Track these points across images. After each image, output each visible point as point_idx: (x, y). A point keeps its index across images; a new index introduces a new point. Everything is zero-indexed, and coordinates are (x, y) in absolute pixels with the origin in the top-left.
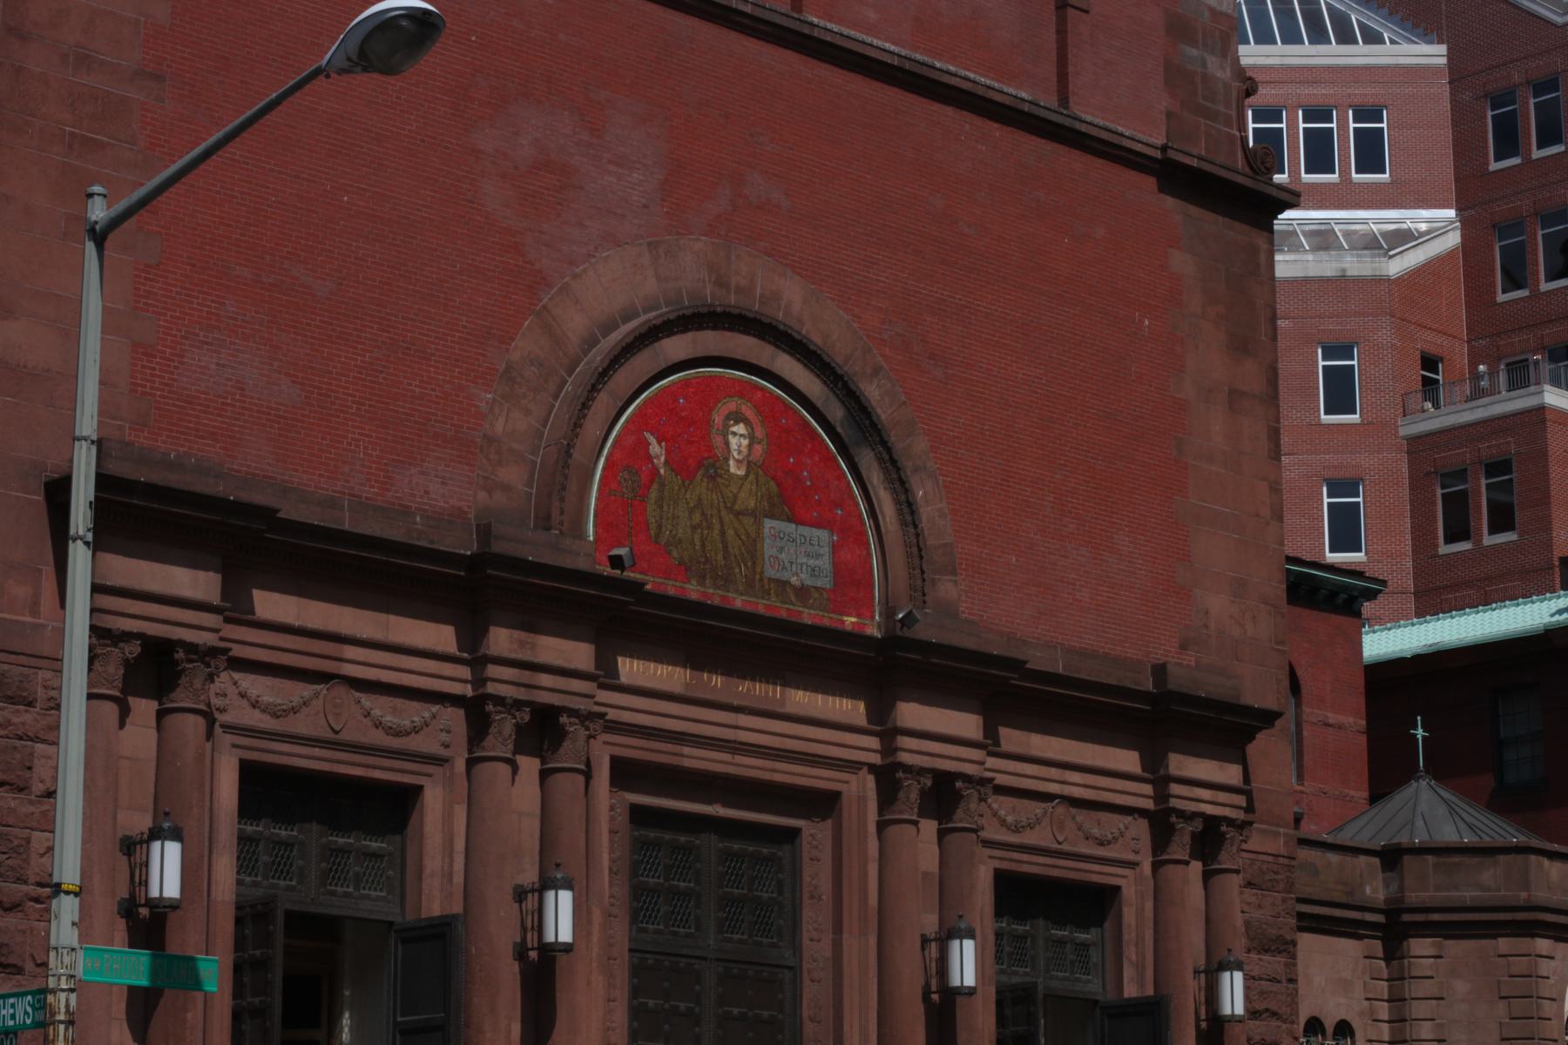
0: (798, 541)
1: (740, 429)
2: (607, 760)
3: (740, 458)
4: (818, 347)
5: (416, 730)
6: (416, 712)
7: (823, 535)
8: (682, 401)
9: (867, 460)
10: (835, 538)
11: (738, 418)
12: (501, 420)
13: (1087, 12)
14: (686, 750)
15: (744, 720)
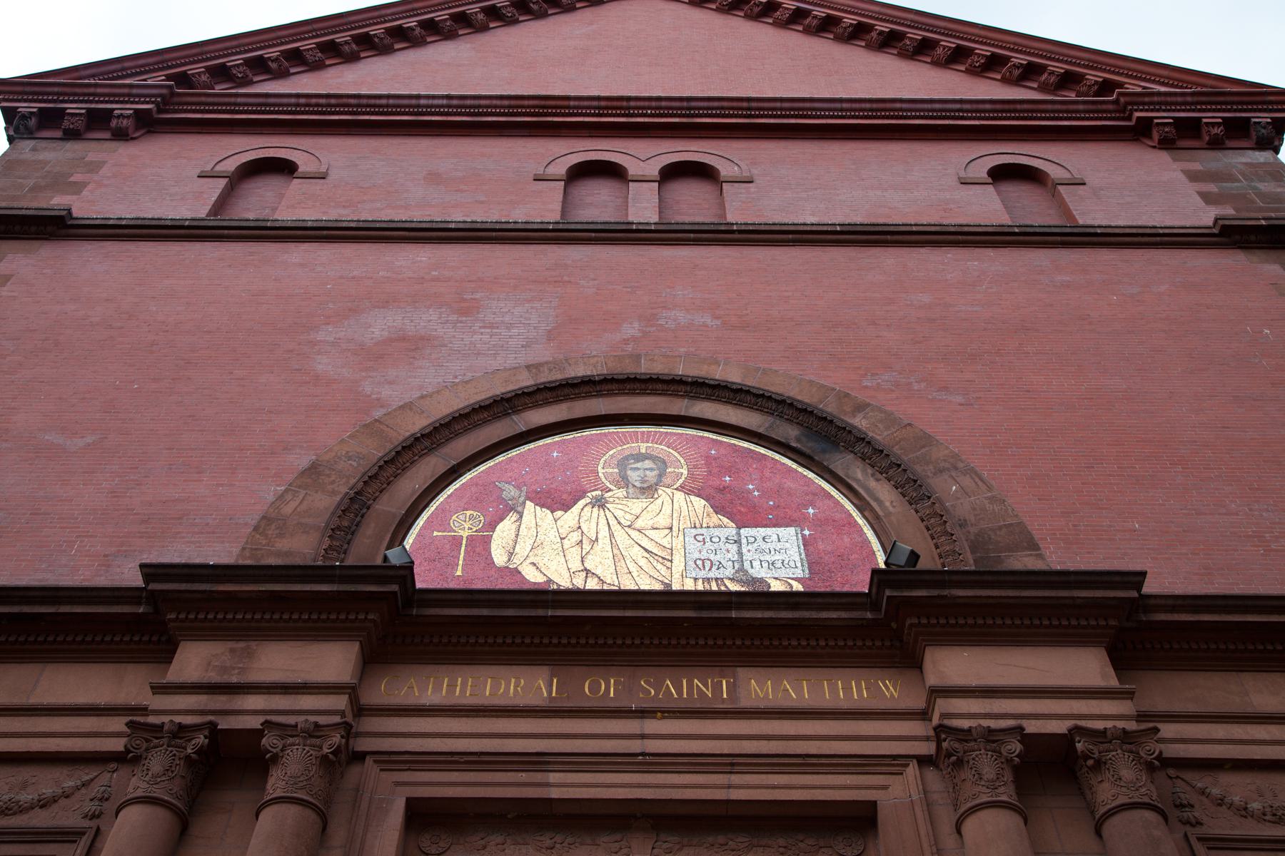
0: (744, 541)
1: (648, 464)
2: (400, 805)
3: (645, 485)
4: (740, 384)
5: (44, 804)
6: (46, 781)
7: (789, 533)
8: (555, 454)
9: (843, 463)
10: (807, 532)
11: (640, 457)
12: (293, 505)
13: (1085, 184)
14: (553, 777)
15: (652, 726)
